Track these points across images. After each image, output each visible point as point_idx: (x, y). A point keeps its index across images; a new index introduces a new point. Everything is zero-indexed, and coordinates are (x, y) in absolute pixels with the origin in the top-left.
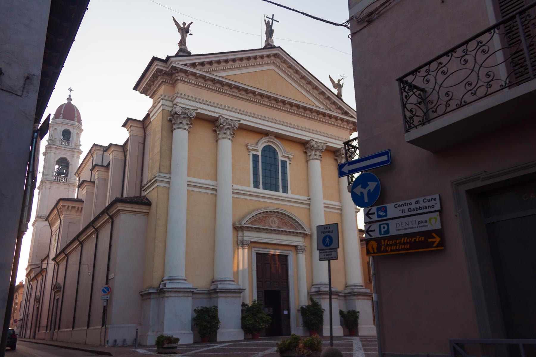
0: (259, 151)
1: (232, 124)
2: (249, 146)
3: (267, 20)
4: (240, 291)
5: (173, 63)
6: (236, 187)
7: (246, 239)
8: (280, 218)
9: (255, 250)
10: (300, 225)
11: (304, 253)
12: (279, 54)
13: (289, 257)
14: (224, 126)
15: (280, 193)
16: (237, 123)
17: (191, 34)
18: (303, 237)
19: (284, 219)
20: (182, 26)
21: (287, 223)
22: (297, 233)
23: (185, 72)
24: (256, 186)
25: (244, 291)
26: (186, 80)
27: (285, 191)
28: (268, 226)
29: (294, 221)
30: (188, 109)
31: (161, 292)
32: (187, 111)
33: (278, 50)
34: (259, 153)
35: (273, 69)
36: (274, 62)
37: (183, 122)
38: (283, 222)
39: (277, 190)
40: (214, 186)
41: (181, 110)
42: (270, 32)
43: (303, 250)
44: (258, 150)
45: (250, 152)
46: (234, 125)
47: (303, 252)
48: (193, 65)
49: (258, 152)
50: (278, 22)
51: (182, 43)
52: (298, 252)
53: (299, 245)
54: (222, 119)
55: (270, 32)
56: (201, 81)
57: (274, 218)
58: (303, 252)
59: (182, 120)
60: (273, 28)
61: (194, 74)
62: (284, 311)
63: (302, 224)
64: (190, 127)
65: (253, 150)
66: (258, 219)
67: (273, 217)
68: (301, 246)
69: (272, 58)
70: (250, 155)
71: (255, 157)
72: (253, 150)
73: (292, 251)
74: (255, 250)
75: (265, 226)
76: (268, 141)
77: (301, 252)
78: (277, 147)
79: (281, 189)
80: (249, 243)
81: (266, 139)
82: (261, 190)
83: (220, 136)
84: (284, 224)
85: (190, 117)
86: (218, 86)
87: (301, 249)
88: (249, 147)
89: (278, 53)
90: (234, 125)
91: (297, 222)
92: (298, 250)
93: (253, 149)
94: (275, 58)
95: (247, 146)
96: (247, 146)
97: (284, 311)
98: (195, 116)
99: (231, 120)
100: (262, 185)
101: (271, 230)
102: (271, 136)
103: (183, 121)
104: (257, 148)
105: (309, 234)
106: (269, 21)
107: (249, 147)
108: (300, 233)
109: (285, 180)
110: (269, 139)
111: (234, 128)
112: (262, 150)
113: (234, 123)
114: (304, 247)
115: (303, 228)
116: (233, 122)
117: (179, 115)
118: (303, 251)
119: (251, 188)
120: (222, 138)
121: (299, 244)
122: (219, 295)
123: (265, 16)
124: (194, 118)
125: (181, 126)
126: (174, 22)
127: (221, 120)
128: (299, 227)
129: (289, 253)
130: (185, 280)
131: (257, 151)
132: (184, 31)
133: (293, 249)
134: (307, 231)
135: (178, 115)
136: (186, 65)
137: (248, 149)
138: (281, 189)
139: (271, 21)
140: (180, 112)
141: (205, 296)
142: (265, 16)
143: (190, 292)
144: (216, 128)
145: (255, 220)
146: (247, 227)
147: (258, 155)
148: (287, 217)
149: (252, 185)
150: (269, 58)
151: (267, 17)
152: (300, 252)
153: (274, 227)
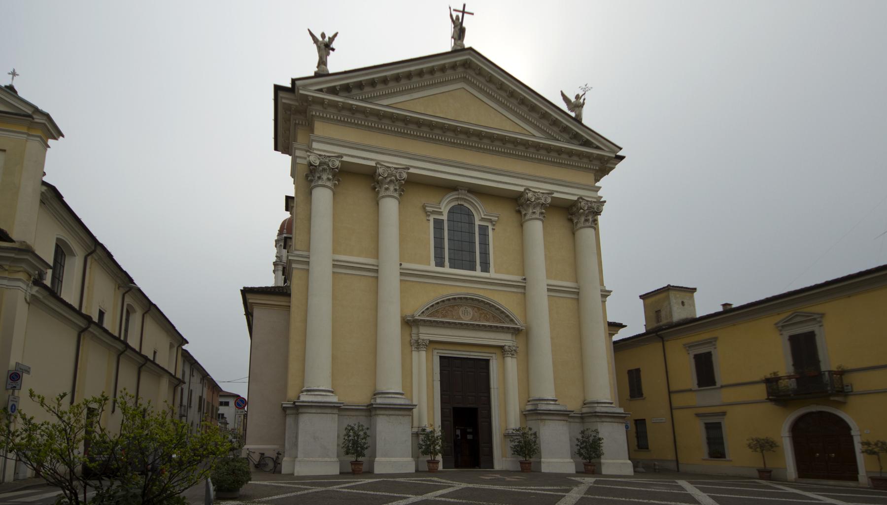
0: (444, 214)
1: (398, 175)
2: (428, 207)
3: (454, 14)
4: (407, 410)
5: (301, 90)
6: (405, 265)
7: (422, 337)
8: (476, 307)
9: (437, 353)
10: (508, 316)
11: (514, 356)
12: (471, 60)
13: (491, 361)
14: (385, 178)
15: (478, 273)
16: (405, 172)
17: (325, 47)
18: (512, 334)
19: (482, 309)
20: (320, 39)
21: (487, 314)
22: (502, 327)
23: (321, 102)
24: (440, 263)
25: (415, 407)
26: (325, 115)
27: (485, 268)
28: (457, 319)
29: (502, 314)
30: (329, 157)
31: (297, 408)
32: (327, 160)
33: (470, 54)
34: (445, 217)
35: (463, 88)
36: (465, 75)
37: (323, 177)
38: (481, 314)
39: (474, 269)
40: (373, 265)
41: (319, 159)
42: (460, 32)
43: (513, 352)
44: (442, 212)
45: (429, 216)
46: (400, 176)
47: (512, 355)
48: (333, 91)
49: (443, 215)
50: (472, 14)
51: (322, 62)
52: (506, 355)
53: (505, 345)
54: (380, 167)
55: (460, 32)
56: (347, 114)
57: (467, 307)
58: (512, 355)
59: (321, 174)
60: (464, 25)
61: (334, 105)
62: (472, 438)
63: (510, 315)
64: (335, 184)
65: (434, 212)
66: (442, 309)
67: (465, 307)
68: (509, 346)
69: (460, 70)
70: (429, 220)
71: (438, 224)
72: (434, 212)
73: (495, 354)
74: (437, 353)
75: (453, 318)
76: (458, 198)
77: (510, 355)
78: (471, 205)
79: (478, 267)
80: (428, 342)
81: (453, 195)
82: (447, 269)
83: (382, 193)
84: (483, 316)
85: (333, 169)
86: (373, 120)
87: (509, 351)
88: (428, 209)
89: (469, 59)
90: (400, 176)
91: (503, 312)
92: (506, 353)
93: (433, 211)
94: (466, 68)
95: (424, 207)
96: (424, 207)
97: (472, 438)
98: (340, 166)
99: (396, 168)
100: (449, 262)
101: (461, 324)
102: (461, 190)
103: (322, 175)
104: (440, 209)
105: (522, 330)
106: (457, 17)
107: (427, 208)
108: (508, 328)
109: (485, 254)
110: (458, 195)
111: (400, 180)
112: (449, 212)
113: (399, 172)
114: (514, 348)
115: (512, 320)
116: (399, 171)
117: (316, 166)
118: (513, 353)
119: (432, 267)
120: (383, 197)
121: (507, 344)
122: (378, 412)
123: (450, 8)
124: (339, 169)
125: (320, 183)
126: (311, 38)
127: (380, 169)
128: (507, 319)
129: (492, 357)
130: (332, 392)
131: (441, 213)
132: (325, 47)
133: (498, 351)
134: (519, 324)
135: (314, 167)
136: (321, 90)
137: (426, 212)
138: (478, 267)
139: (460, 15)
140: (317, 163)
141: (363, 413)
142: (450, 8)
143: (338, 408)
144: (376, 183)
145: (437, 311)
146: (424, 321)
147: (443, 220)
148: (493, 309)
149: (433, 262)
150: (455, 70)
151: (455, 10)
152: (508, 355)
153: (466, 320)
